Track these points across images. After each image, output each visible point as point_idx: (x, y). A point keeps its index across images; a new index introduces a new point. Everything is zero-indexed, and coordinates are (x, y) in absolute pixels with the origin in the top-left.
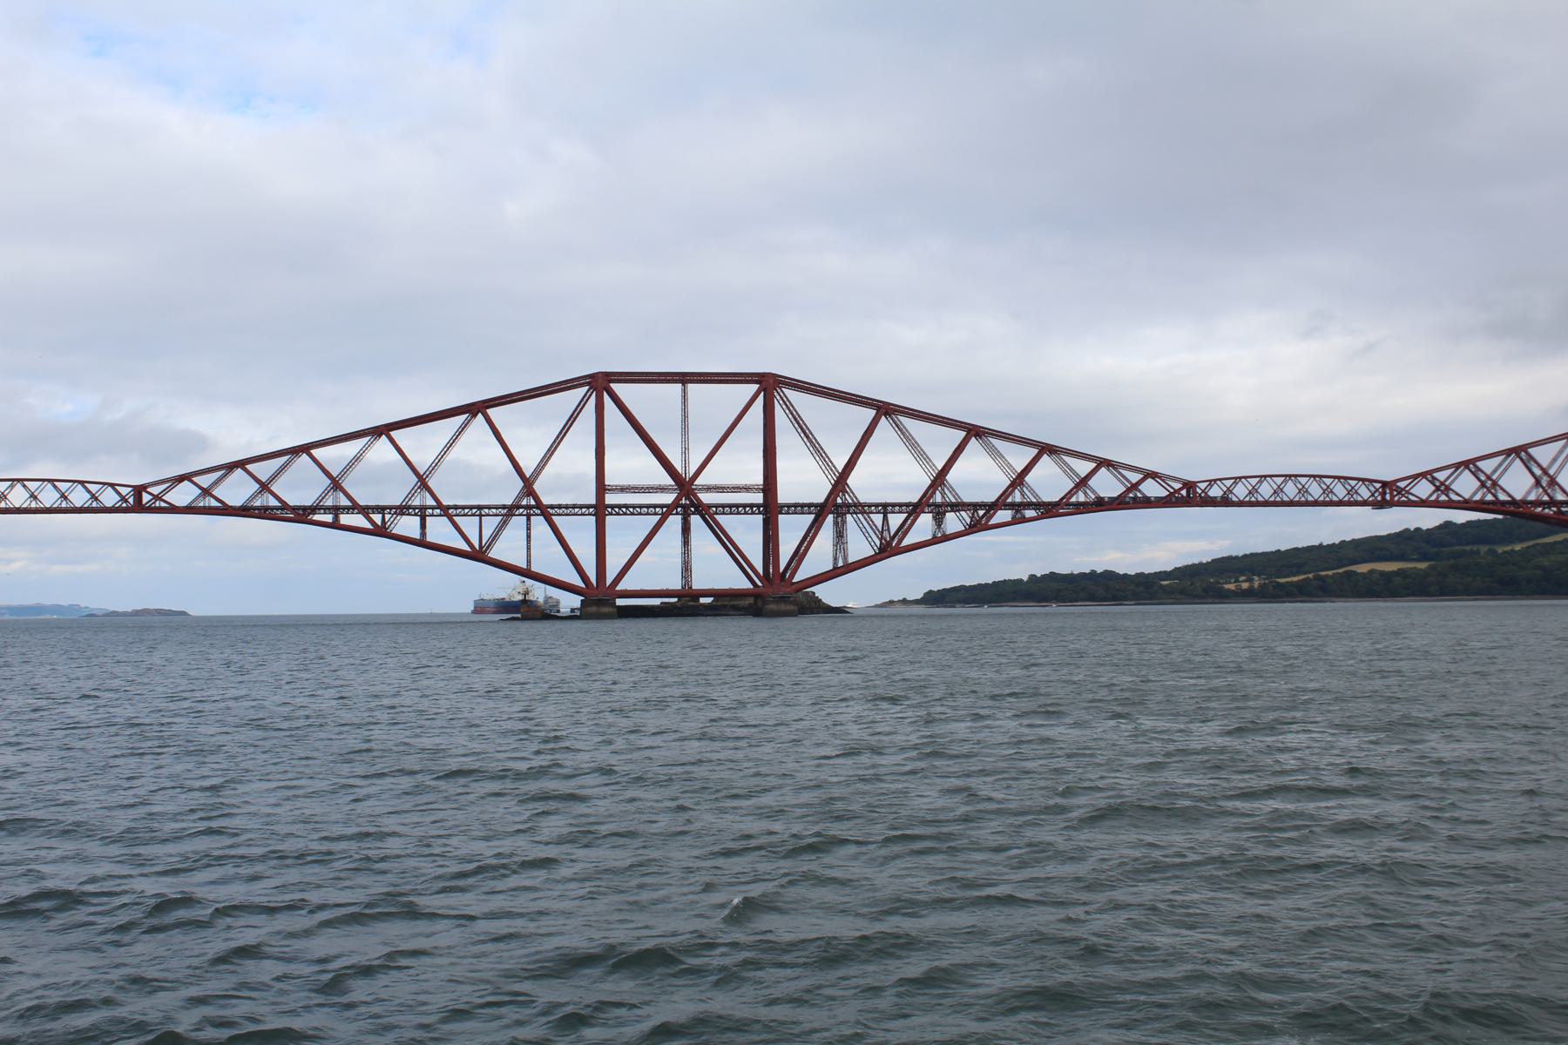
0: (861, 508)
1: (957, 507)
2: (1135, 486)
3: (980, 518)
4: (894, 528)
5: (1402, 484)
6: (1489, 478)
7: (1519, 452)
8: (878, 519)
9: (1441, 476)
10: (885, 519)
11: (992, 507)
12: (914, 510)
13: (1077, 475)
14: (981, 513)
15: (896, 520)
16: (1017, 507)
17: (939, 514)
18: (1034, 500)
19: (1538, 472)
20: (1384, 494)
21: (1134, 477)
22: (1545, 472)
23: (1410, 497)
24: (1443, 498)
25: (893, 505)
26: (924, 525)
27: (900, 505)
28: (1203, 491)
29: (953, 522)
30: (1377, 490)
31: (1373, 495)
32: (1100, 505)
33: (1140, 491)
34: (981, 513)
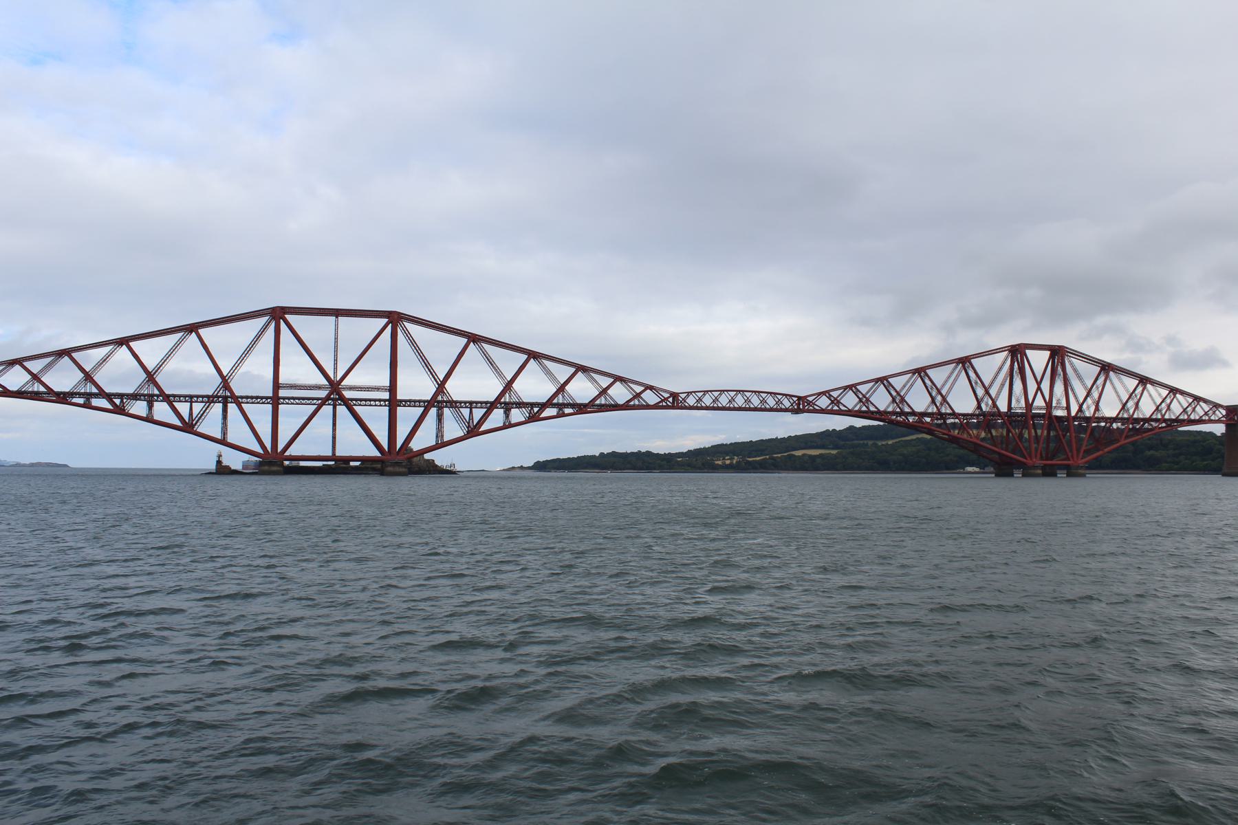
0: (453, 404)
1: (520, 405)
2: (638, 395)
3: (535, 412)
4: (476, 419)
5: (810, 399)
6: (864, 396)
7: (883, 380)
8: (466, 412)
9: (835, 394)
10: (471, 412)
11: (543, 406)
12: (491, 406)
13: (601, 387)
14: (536, 410)
15: (478, 413)
16: (561, 406)
17: (508, 408)
18: (571, 402)
19: (894, 393)
20: (799, 404)
21: (638, 389)
22: (898, 393)
23: (815, 407)
24: (836, 408)
25: (477, 403)
26: (497, 416)
27: (481, 403)
28: (683, 399)
29: (517, 415)
30: (795, 402)
31: (792, 405)
32: (616, 407)
33: (642, 398)
34: (536, 410)
